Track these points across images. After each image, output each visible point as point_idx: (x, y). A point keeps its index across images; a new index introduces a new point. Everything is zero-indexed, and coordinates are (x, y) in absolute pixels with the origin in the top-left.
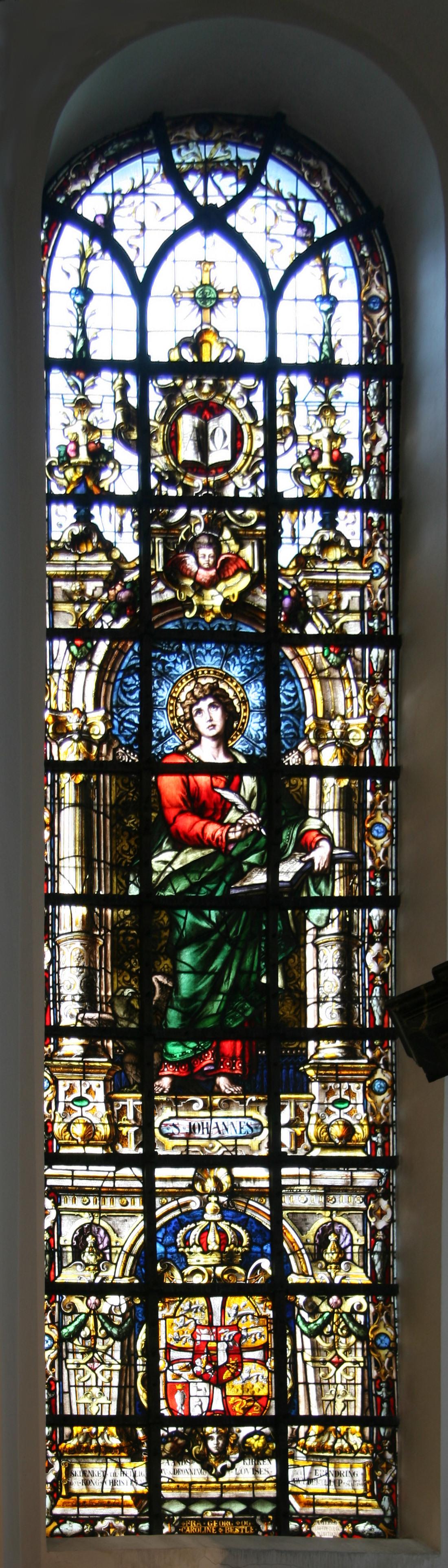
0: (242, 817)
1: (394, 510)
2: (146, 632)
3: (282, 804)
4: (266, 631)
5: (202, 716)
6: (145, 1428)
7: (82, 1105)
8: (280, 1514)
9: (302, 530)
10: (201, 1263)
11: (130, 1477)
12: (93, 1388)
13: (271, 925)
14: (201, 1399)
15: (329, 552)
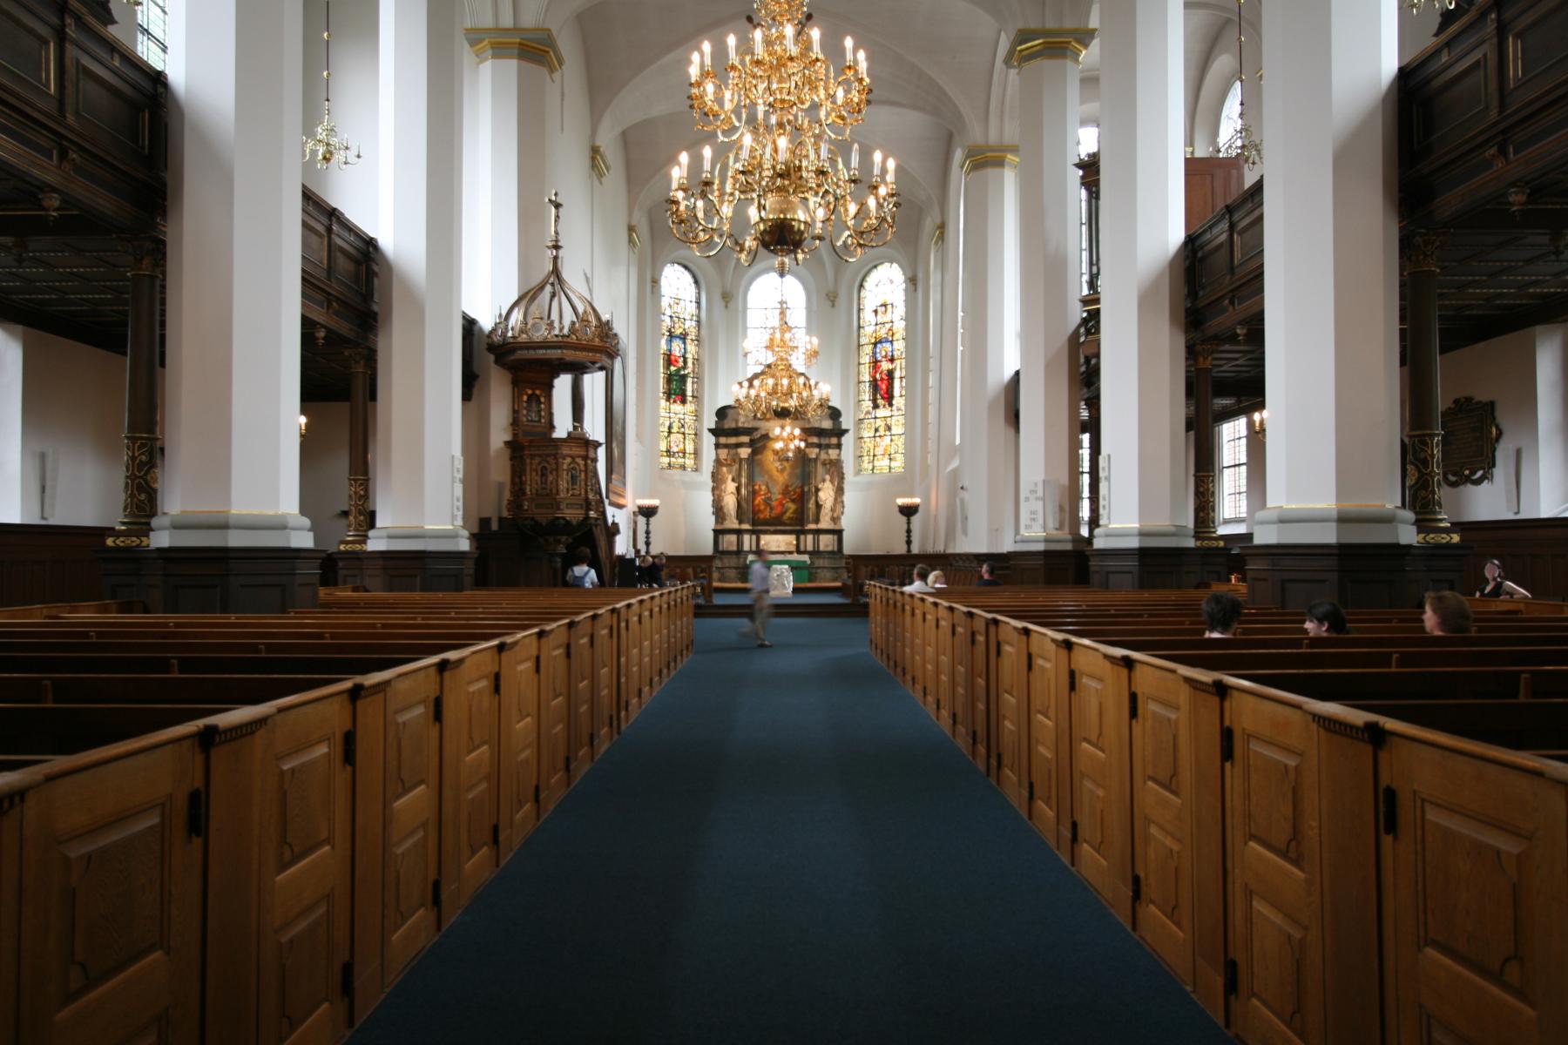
0: (681, 364)
1: (698, 322)
2: (671, 336)
3: (685, 362)
4: (683, 337)
5: (677, 348)
6: (669, 453)
7: (663, 403)
8: (683, 467)
9: (688, 324)
10: (675, 429)
11: (666, 460)
12: (663, 447)
13: (684, 377)
14: (675, 449)
15: (690, 325)
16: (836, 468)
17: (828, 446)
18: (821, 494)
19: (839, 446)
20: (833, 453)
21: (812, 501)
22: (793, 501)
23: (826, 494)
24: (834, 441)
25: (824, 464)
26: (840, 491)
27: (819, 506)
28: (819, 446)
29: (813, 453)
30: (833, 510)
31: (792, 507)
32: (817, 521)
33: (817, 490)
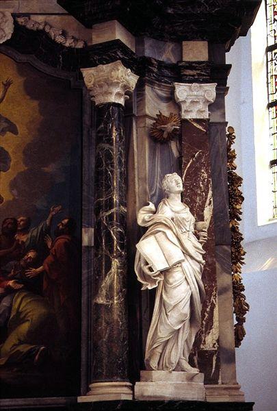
16: (206, 156)
17: (179, 72)
18: (152, 251)
19: (217, 73)
20: (193, 99)
21: (113, 276)
22: (33, 287)
23: (170, 247)
24: (196, 51)
25: (158, 138)
26: (223, 245)
27: (140, 299)
28: (139, 65)
29: (114, 83)
30: (200, 318)
31: (30, 310)
32: (135, 368)
33: (136, 233)
